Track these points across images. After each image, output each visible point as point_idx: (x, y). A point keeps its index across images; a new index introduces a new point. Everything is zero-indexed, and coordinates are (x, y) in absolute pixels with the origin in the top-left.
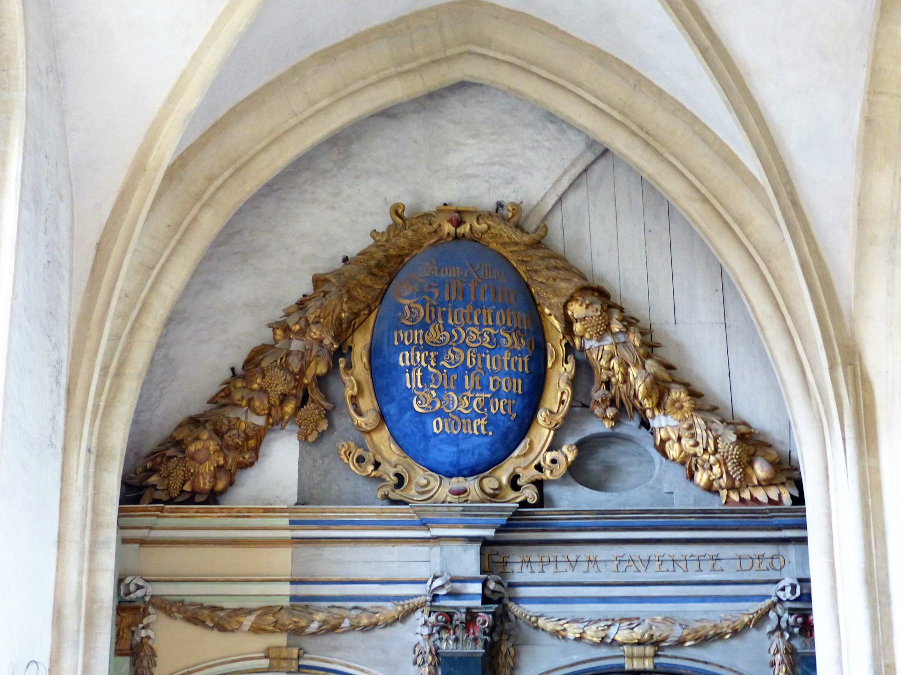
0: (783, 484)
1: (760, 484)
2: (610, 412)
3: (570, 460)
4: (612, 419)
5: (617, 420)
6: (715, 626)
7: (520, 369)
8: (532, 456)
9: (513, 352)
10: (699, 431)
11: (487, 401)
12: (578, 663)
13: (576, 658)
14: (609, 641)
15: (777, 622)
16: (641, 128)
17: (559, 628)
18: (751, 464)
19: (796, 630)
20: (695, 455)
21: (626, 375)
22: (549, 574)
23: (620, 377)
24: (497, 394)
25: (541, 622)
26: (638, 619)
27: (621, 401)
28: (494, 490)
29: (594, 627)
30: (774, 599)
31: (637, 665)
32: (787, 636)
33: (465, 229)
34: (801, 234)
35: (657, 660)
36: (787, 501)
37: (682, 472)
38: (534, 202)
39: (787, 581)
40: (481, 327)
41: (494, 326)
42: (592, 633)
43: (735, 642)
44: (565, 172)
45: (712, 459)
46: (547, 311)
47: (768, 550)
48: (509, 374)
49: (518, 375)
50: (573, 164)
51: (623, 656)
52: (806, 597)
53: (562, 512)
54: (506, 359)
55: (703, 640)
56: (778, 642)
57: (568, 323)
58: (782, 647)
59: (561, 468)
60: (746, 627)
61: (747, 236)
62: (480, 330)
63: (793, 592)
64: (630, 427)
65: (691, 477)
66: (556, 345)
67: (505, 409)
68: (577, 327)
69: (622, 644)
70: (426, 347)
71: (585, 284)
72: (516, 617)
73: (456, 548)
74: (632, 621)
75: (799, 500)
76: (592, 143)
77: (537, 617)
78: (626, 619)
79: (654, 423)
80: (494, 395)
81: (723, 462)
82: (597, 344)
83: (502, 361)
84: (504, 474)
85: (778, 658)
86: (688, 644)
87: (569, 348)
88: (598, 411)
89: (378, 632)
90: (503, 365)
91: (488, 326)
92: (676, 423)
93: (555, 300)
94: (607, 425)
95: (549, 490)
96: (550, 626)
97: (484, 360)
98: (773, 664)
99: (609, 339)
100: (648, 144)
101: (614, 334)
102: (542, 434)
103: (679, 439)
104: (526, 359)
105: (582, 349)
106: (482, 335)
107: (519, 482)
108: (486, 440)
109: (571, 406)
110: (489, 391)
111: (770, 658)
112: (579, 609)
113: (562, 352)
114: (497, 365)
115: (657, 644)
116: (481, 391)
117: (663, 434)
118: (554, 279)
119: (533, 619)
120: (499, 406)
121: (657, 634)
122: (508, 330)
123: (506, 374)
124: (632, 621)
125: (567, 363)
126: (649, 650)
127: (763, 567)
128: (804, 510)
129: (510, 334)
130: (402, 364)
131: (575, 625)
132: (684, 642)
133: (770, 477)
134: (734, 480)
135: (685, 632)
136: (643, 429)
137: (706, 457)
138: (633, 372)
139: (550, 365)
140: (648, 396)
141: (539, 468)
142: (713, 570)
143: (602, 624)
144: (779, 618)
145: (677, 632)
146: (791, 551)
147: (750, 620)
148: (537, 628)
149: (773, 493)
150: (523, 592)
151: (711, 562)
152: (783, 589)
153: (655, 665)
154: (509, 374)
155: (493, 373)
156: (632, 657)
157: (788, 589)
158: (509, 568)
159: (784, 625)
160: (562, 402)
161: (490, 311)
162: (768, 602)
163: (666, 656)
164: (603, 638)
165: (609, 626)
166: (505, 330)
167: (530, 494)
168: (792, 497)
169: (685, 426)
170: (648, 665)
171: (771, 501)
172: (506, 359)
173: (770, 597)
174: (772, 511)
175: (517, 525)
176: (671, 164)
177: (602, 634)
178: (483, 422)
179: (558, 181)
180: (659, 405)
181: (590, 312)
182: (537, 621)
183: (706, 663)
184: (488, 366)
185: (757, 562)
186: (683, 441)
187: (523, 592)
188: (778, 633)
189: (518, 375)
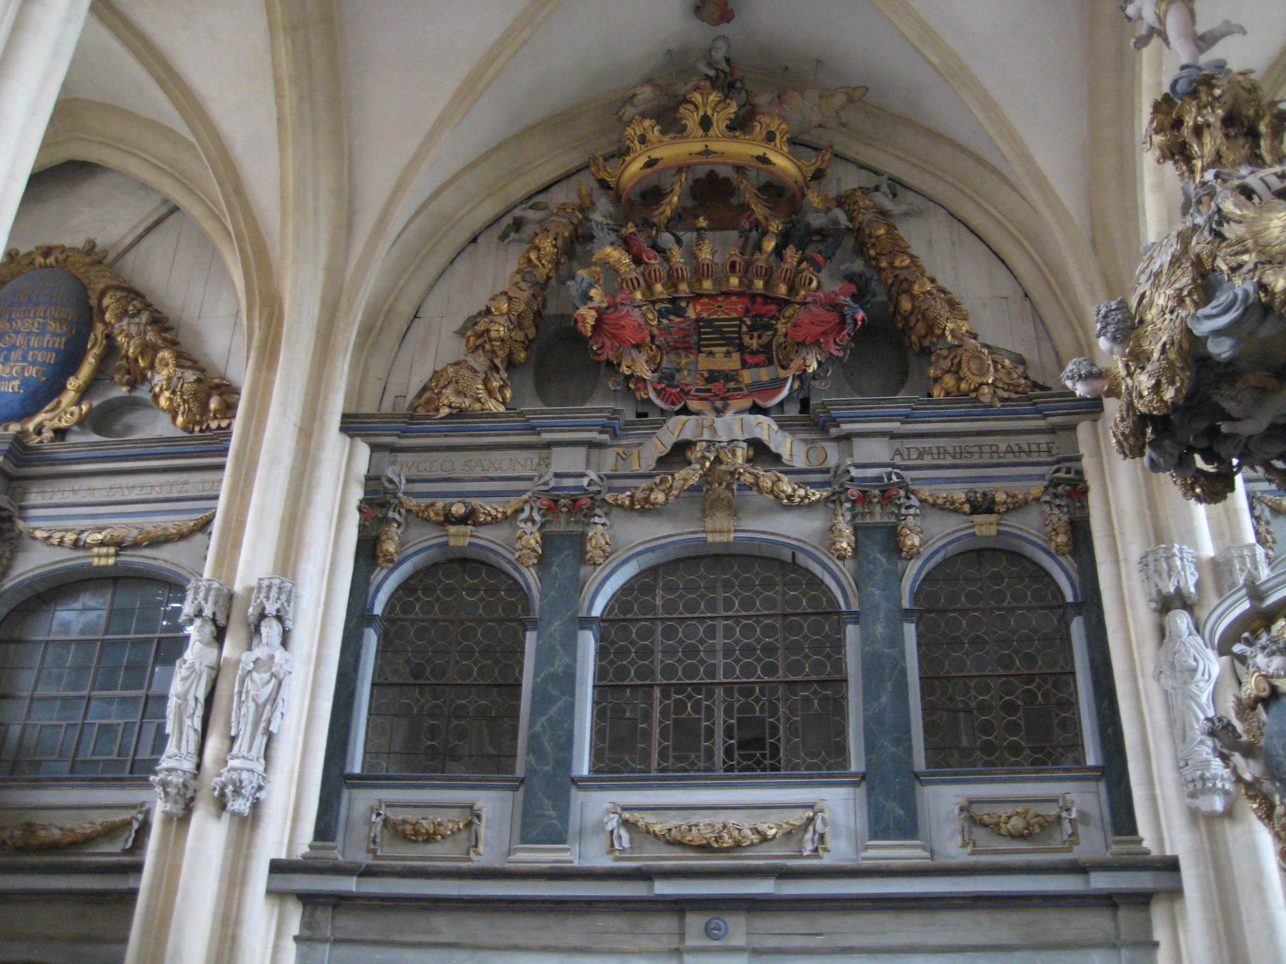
9: (54, 334)
12: (57, 562)
16: (182, 174)
24: (33, 363)
31: (103, 562)
33: (51, 260)
34: (240, 215)
35: (119, 559)
37: (168, 417)
41: (45, 318)
42: (70, 538)
44: (143, 221)
48: (47, 349)
49: (52, 350)
50: (150, 214)
76: (166, 201)
88: (117, 377)
94: (123, 391)
102: (69, 396)
104: (64, 340)
115: (120, 545)
122: (54, 320)
126: (112, 550)
154: (47, 349)
155: (33, 349)
156: (99, 556)
170: (111, 561)
171: (219, 428)
179: (136, 227)
189: (52, 350)
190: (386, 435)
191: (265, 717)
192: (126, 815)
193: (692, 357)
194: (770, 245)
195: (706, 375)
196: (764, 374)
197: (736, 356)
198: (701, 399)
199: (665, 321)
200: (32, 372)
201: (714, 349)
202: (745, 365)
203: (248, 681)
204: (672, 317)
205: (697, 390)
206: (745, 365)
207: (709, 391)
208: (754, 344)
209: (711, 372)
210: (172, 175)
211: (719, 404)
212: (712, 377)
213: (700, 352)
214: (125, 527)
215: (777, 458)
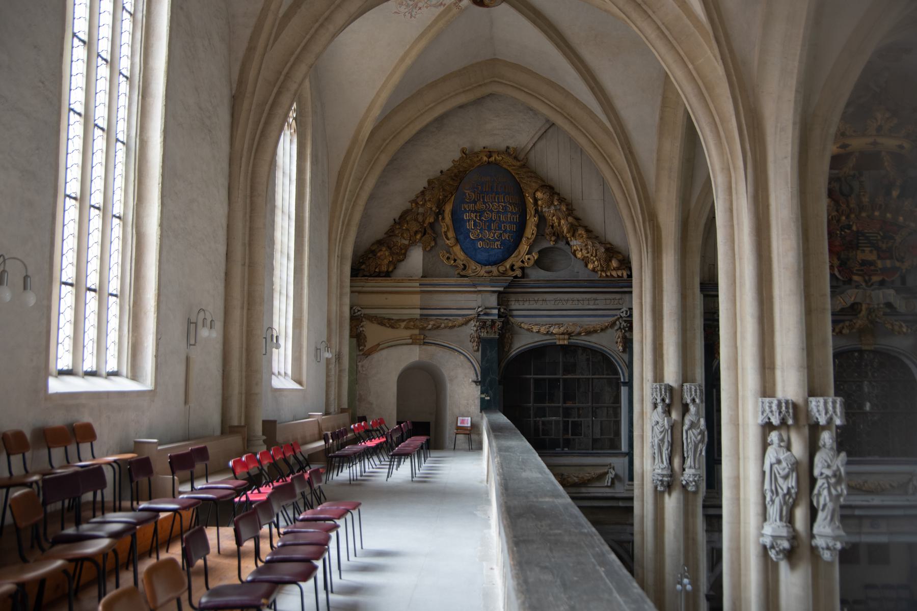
0: (624, 269)
1: (614, 269)
2: (553, 238)
3: (535, 258)
4: (554, 241)
5: (556, 241)
6: (594, 327)
7: (515, 221)
8: (520, 257)
9: (512, 213)
10: (589, 247)
11: (501, 234)
13: (536, 340)
14: (550, 333)
15: (619, 326)
16: (568, 115)
17: (530, 328)
18: (611, 261)
19: (627, 329)
20: (588, 257)
21: (559, 223)
22: (526, 306)
23: (557, 224)
24: (505, 231)
25: (522, 325)
26: (562, 324)
27: (558, 234)
28: (504, 271)
29: (544, 327)
30: (619, 316)
31: (561, 343)
32: (623, 331)
33: (492, 159)
34: (633, 166)
35: (570, 341)
36: (625, 274)
37: (583, 263)
38: (523, 146)
39: (624, 309)
40: (499, 202)
41: (504, 202)
42: (543, 330)
43: (602, 334)
44: (537, 133)
45: (594, 259)
46: (527, 195)
47: (618, 296)
48: (510, 222)
51: (555, 339)
52: (631, 316)
53: (531, 281)
54: (509, 216)
55: (589, 333)
56: (619, 333)
57: (536, 201)
58: (621, 336)
59: (532, 262)
60: (607, 328)
61: (613, 163)
62: (498, 204)
63: (626, 314)
64: (561, 244)
65: (586, 266)
66: (531, 209)
67: (508, 238)
68: (540, 203)
69: (556, 334)
70: (475, 211)
71: (544, 184)
72: (512, 323)
73: (488, 295)
74: (560, 325)
75: (630, 276)
76: (548, 121)
77: (521, 323)
78: (558, 324)
79: (572, 243)
80: (504, 231)
81: (599, 260)
82: (548, 210)
83: (508, 217)
84: (508, 264)
85: (619, 340)
86: (582, 334)
87: (536, 211)
88: (548, 237)
89: (456, 329)
90: (508, 219)
91: (502, 202)
92: (580, 243)
93: (530, 191)
95: (528, 271)
96: (526, 327)
97: (500, 217)
98: (617, 343)
99: (553, 208)
100: (572, 122)
101: (555, 206)
102: (524, 247)
103: (581, 250)
104: (518, 216)
105: (542, 211)
106: (499, 206)
107: (514, 268)
108: (500, 250)
109: (536, 235)
110: (502, 230)
111: (616, 340)
112: (538, 319)
113: (533, 213)
114: (505, 219)
115: (570, 334)
116: (498, 230)
117: (575, 248)
118: (530, 182)
119: (519, 324)
120: (506, 236)
121: (570, 330)
122: (510, 204)
123: (509, 223)
124: (560, 325)
125: (535, 217)
126: (566, 337)
127: (615, 303)
128: (632, 280)
129: (511, 206)
130: (465, 218)
131: (536, 326)
132: (581, 333)
133: (618, 266)
134: (603, 267)
135: (582, 329)
136: (567, 245)
137: (592, 258)
138: (562, 222)
139: (528, 218)
140: (568, 232)
141: (523, 262)
142: (594, 304)
143: (548, 326)
144: (620, 324)
145: (578, 329)
146: (627, 296)
147: (608, 325)
148: (521, 327)
149: (620, 273)
150: (515, 313)
151: (593, 301)
152: (622, 312)
153: (569, 342)
154: (510, 222)
155: (504, 222)
156: (559, 339)
157: (625, 312)
158: (510, 303)
159: (622, 327)
160: (533, 234)
161: (502, 196)
162: (616, 317)
163: (573, 339)
164: (548, 332)
165: (550, 327)
166: (509, 204)
167: (518, 273)
168: (627, 275)
169: (584, 245)
170: (566, 342)
171: (618, 276)
172: (509, 216)
173: (617, 315)
174: (619, 280)
175: (513, 286)
176: (581, 130)
177: (547, 330)
178: (499, 243)
180: (573, 235)
181: (545, 197)
182: (520, 325)
183: (589, 342)
184: (502, 219)
185: (613, 301)
186: (583, 251)
187: (515, 313)
188: (619, 330)
190: (713, 291)
191: (699, 449)
192: (605, 470)
193: (854, 252)
194: (895, 193)
195: (860, 262)
196: (888, 263)
197: (875, 252)
198: (859, 275)
199: (843, 233)
200: (506, 236)
201: (865, 249)
202: (879, 257)
203: (690, 432)
204: (846, 230)
205: (857, 270)
206: (879, 257)
207: (862, 270)
208: (884, 246)
209: (863, 260)
210: (562, 114)
211: (867, 278)
212: (864, 263)
213: (858, 249)
214: (569, 323)
215: (895, 308)
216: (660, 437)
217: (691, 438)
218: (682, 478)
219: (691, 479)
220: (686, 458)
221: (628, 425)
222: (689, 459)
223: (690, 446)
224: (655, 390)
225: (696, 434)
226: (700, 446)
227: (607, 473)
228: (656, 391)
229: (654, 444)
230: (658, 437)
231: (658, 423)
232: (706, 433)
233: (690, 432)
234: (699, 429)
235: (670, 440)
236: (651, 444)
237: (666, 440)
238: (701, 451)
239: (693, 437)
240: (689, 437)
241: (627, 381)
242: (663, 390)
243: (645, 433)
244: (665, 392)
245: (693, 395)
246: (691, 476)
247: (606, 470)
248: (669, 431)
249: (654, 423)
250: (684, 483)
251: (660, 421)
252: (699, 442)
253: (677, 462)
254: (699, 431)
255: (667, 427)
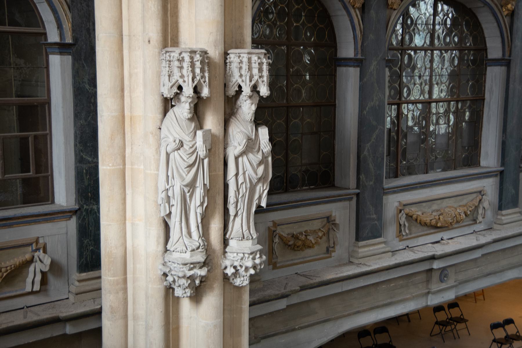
191: (257, 196)
216: (189, 178)
217: (244, 173)
218: (227, 263)
219: (249, 264)
220: (232, 218)
221: (75, 145)
222: (238, 220)
223: (243, 190)
224: (177, 63)
225: (255, 165)
226: (258, 188)
227: (31, 261)
228: (181, 68)
229: (170, 193)
230: (183, 179)
231: (181, 144)
232: (270, 159)
233: (244, 161)
234: (261, 152)
235: (207, 182)
236: (163, 195)
237: (199, 184)
238: (260, 198)
239: (250, 171)
240: (241, 172)
241: (69, 40)
242: (198, 65)
243: (128, 166)
244: (202, 70)
245: (198, 78)
246: (247, 255)
247: (28, 256)
248: (206, 161)
249: (172, 146)
250: (230, 271)
251: (187, 139)
252: (259, 180)
253: (216, 226)
254: (260, 156)
255: (202, 152)
